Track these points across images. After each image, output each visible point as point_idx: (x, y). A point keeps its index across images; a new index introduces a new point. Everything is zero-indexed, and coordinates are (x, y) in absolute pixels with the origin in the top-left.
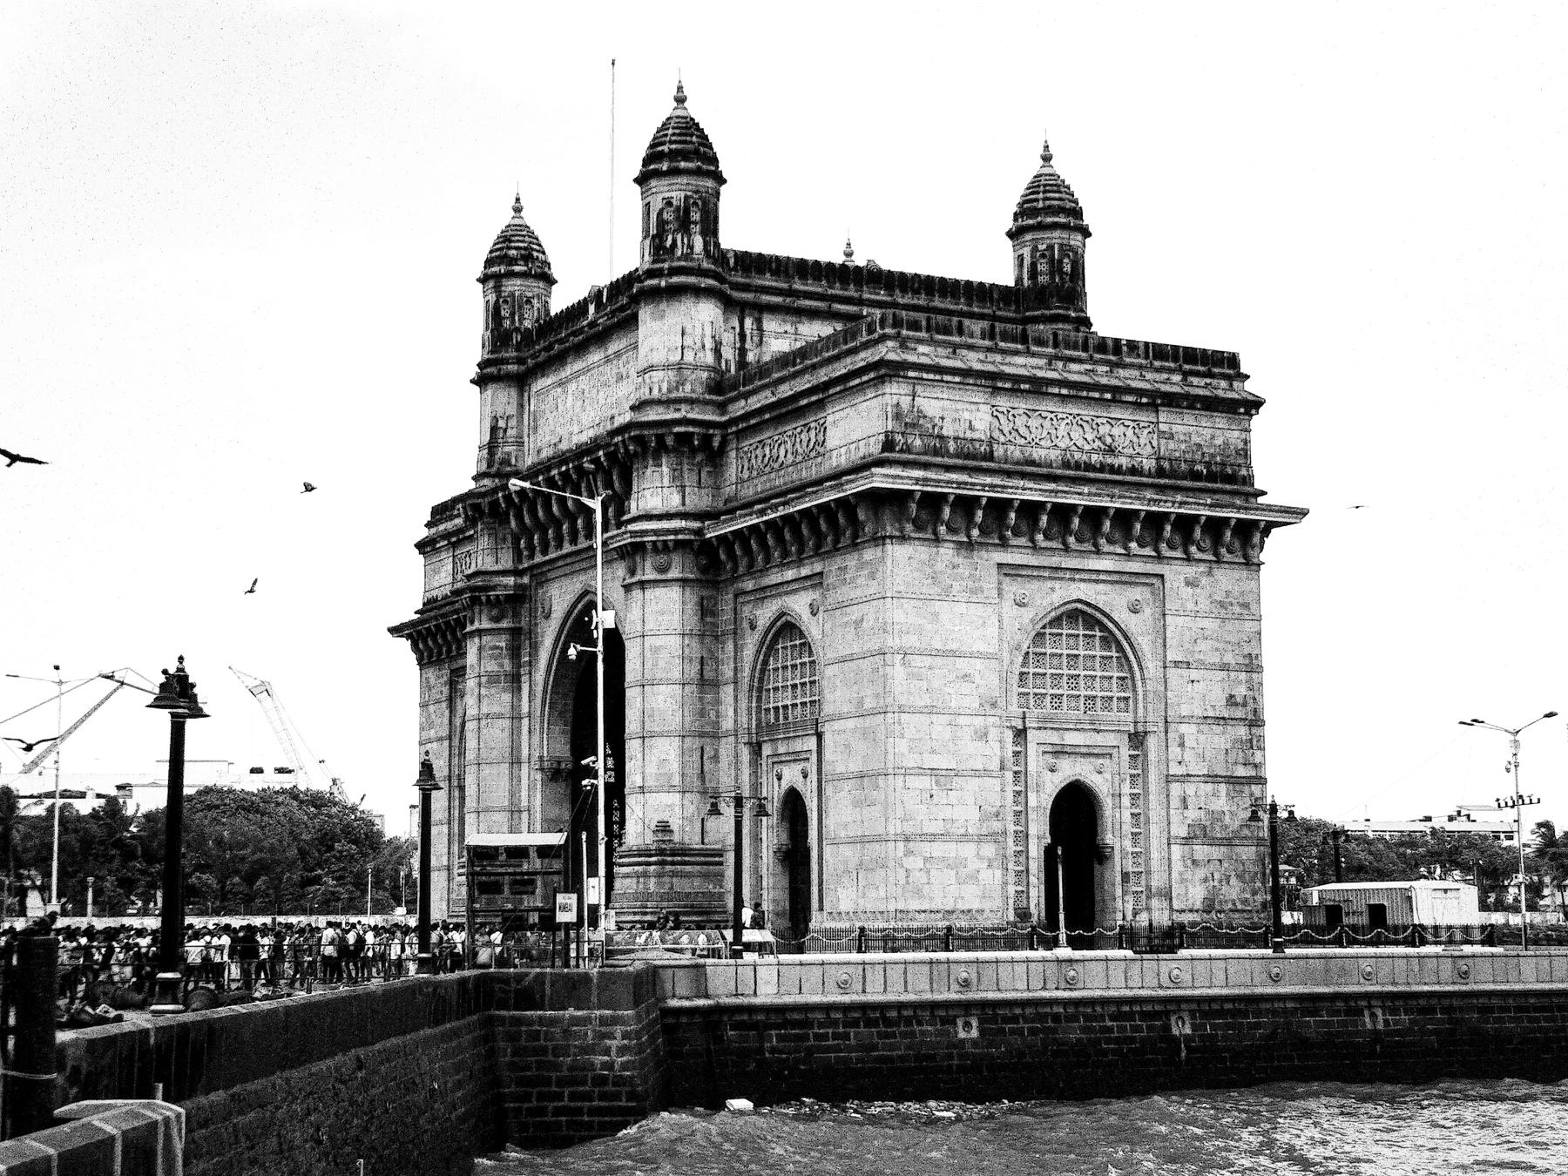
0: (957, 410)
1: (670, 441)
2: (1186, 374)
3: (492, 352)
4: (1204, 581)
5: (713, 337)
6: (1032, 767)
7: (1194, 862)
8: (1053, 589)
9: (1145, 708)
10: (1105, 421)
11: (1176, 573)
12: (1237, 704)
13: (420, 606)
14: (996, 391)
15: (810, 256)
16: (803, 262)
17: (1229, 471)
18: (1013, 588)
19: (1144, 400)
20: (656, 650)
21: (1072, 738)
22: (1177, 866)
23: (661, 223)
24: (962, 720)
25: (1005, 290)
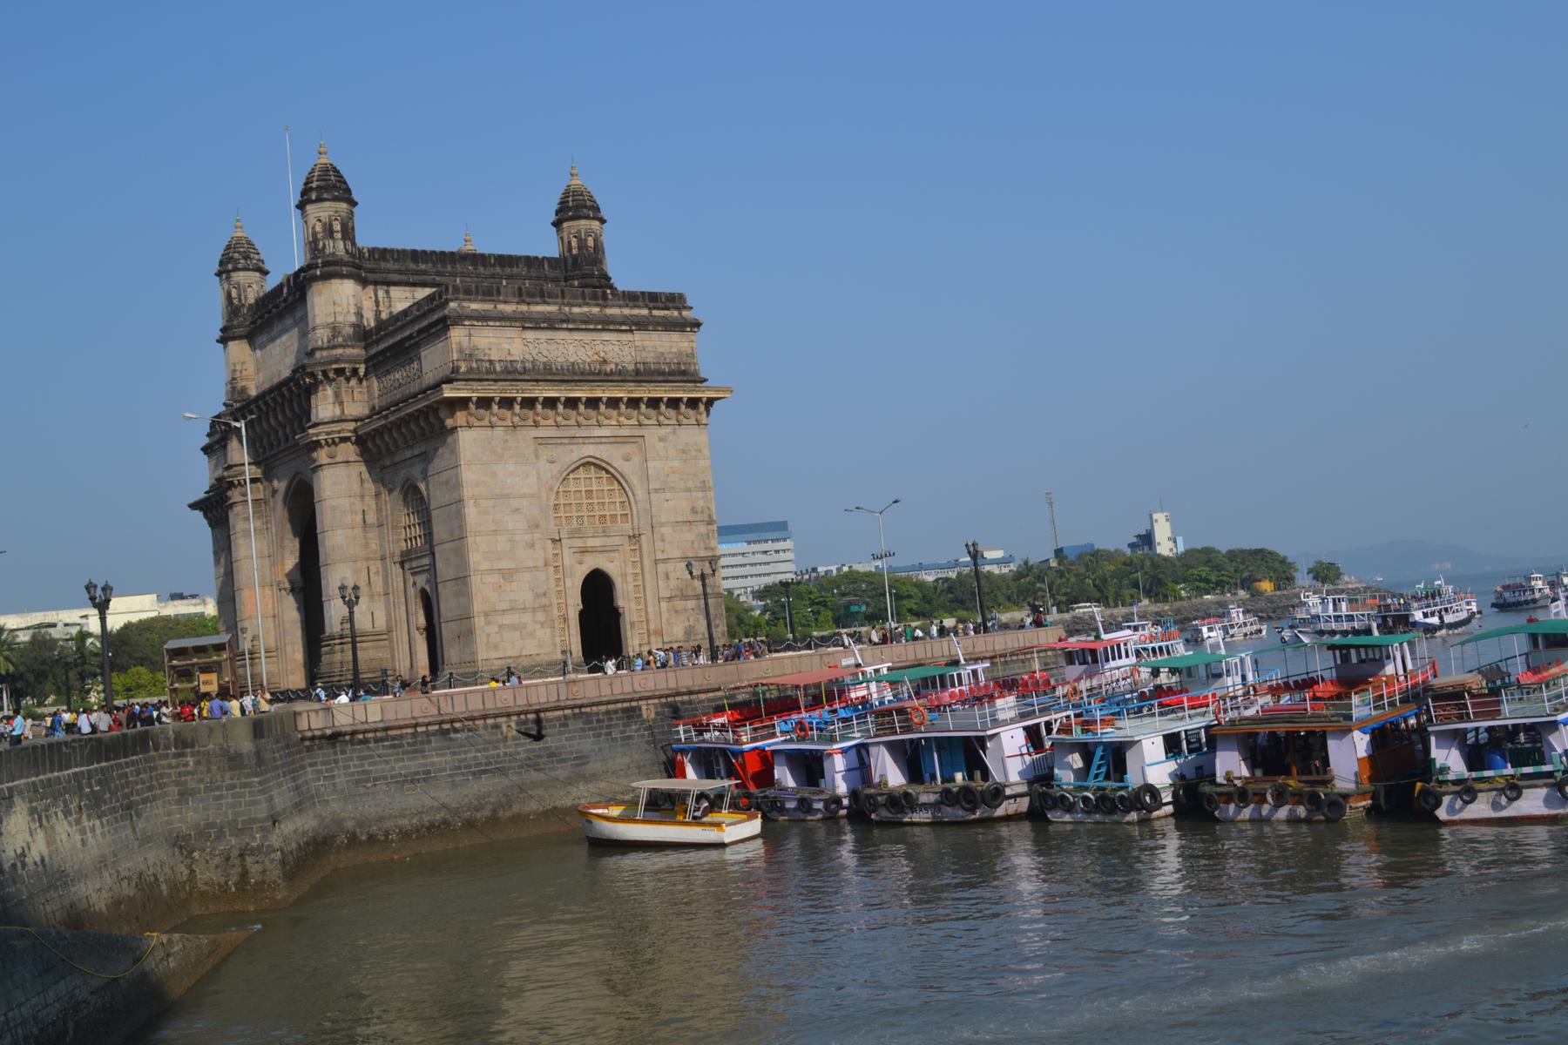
0: (500, 344)
1: (331, 375)
2: (650, 309)
3: (228, 321)
4: (671, 437)
5: (356, 305)
6: (567, 562)
7: (676, 612)
8: (572, 451)
9: (639, 519)
11: (652, 434)
12: (697, 513)
13: (208, 489)
14: (524, 328)
15: (419, 248)
16: (414, 252)
17: (683, 368)
18: (546, 453)
19: (624, 328)
20: (334, 508)
21: (591, 542)
22: (665, 615)
23: (315, 234)
25: (550, 260)
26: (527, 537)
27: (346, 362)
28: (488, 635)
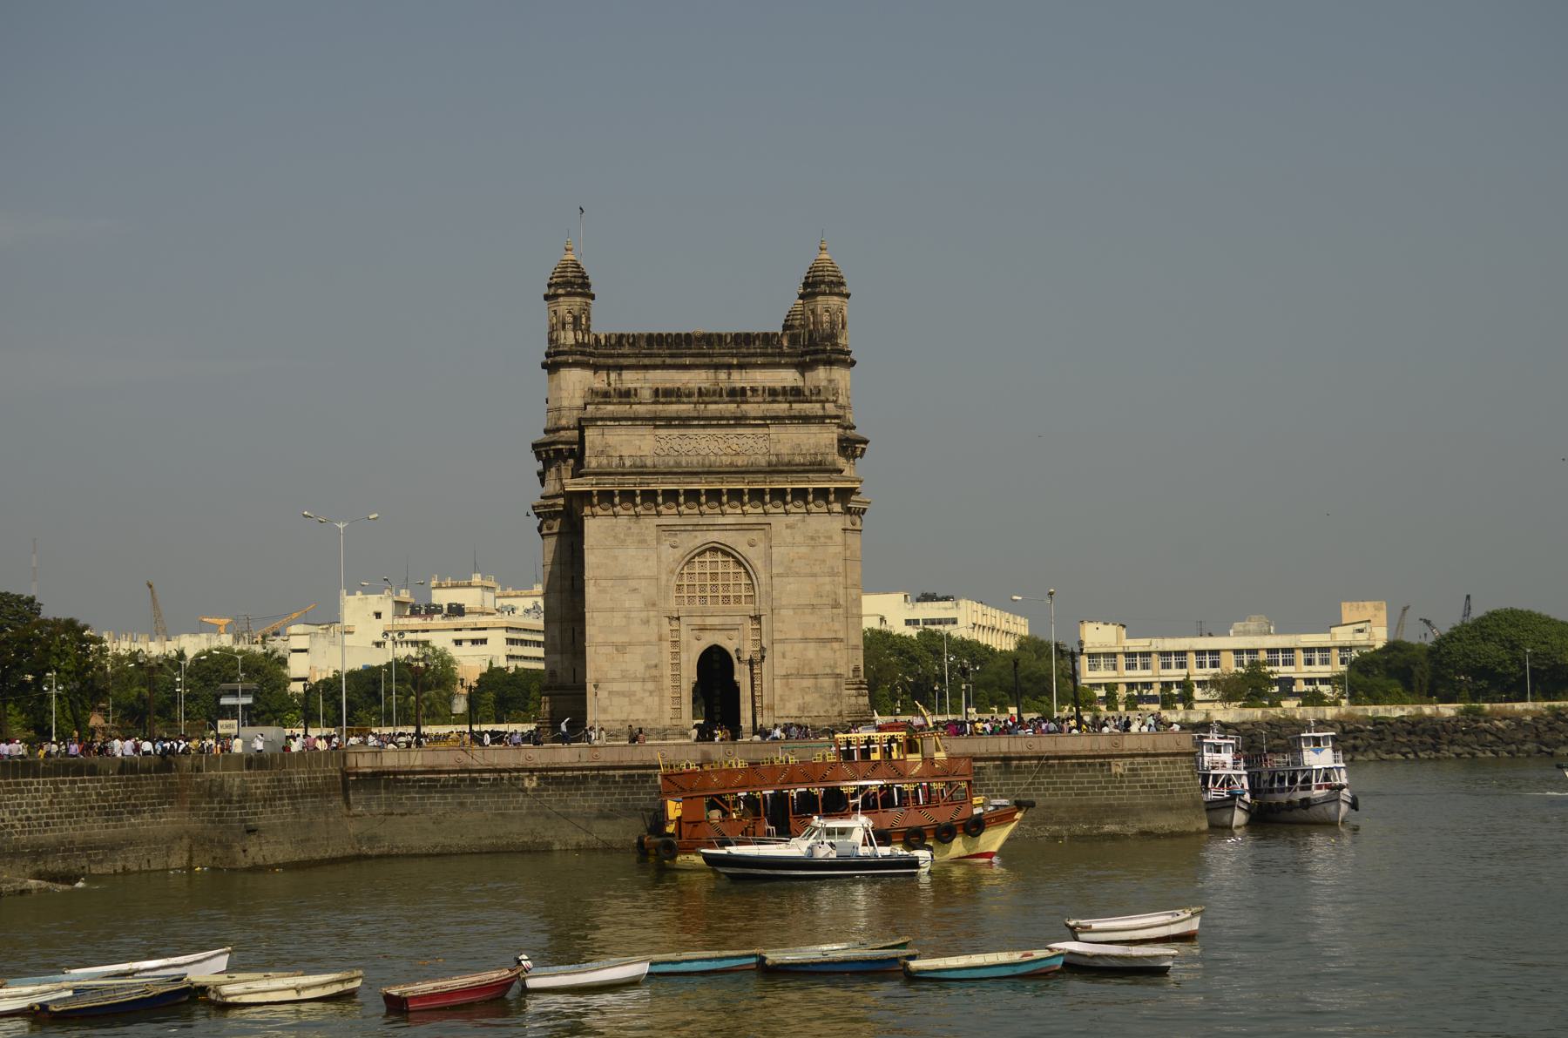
8: (696, 537)
10: (733, 436)
12: (821, 596)
14: (656, 427)
17: (819, 458)
18: (668, 540)
21: (709, 621)
22: (778, 692)
24: (633, 615)
26: (644, 615)
27: (562, 443)
28: (599, 699)
